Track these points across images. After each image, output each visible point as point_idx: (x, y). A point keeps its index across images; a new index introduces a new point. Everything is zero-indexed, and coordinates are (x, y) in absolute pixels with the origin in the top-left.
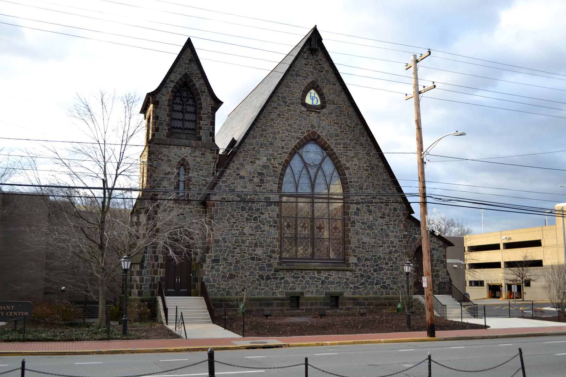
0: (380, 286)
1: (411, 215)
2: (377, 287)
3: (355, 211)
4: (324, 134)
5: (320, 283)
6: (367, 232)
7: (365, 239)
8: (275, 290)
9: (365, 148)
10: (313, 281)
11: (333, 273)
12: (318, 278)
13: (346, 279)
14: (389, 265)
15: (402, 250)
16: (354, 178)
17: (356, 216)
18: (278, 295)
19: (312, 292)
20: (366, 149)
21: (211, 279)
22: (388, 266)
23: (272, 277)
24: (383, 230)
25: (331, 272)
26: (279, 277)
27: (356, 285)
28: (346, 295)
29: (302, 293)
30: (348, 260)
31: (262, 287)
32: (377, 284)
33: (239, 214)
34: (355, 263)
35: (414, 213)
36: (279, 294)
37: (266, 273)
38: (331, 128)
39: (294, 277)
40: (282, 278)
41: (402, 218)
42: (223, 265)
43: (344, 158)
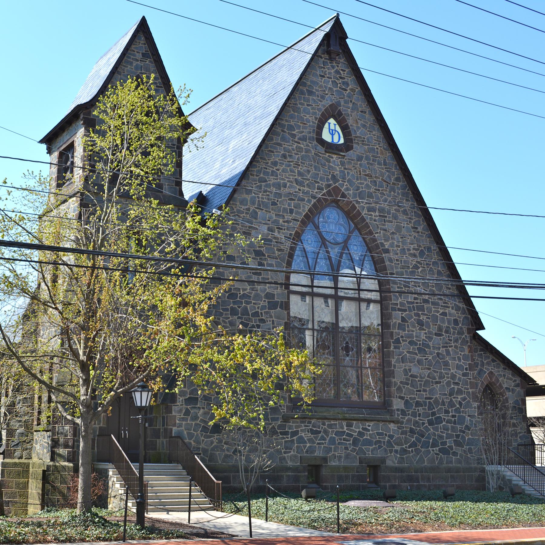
0: (438, 448)
1: (478, 332)
2: (433, 450)
3: (399, 323)
4: (351, 192)
5: (351, 442)
6: (417, 357)
7: (415, 370)
8: (285, 453)
9: (410, 218)
10: (341, 439)
11: (370, 425)
12: (348, 435)
13: (389, 437)
14: (451, 414)
15: (468, 389)
16: (397, 268)
17: (401, 332)
18: (289, 462)
19: (340, 457)
20: (412, 221)
21: (185, 433)
22: (448, 416)
23: (279, 431)
24: (441, 356)
25: (367, 424)
26: (290, 431)
27: (404, 447)
28: (389, 463)
29: (325, 459)
30: (390, 404)
31: (264, 448)
32: (434, 445)
33: (227, 321)
34: (402, 410)
35: (483, 328)
36: (291, 460)
37: (271, 424)
38: (361, 184)
39: (312, 432)
40: (295, 433)
41: (466, 336)
42: (203, 408)
43: (382, 234)
